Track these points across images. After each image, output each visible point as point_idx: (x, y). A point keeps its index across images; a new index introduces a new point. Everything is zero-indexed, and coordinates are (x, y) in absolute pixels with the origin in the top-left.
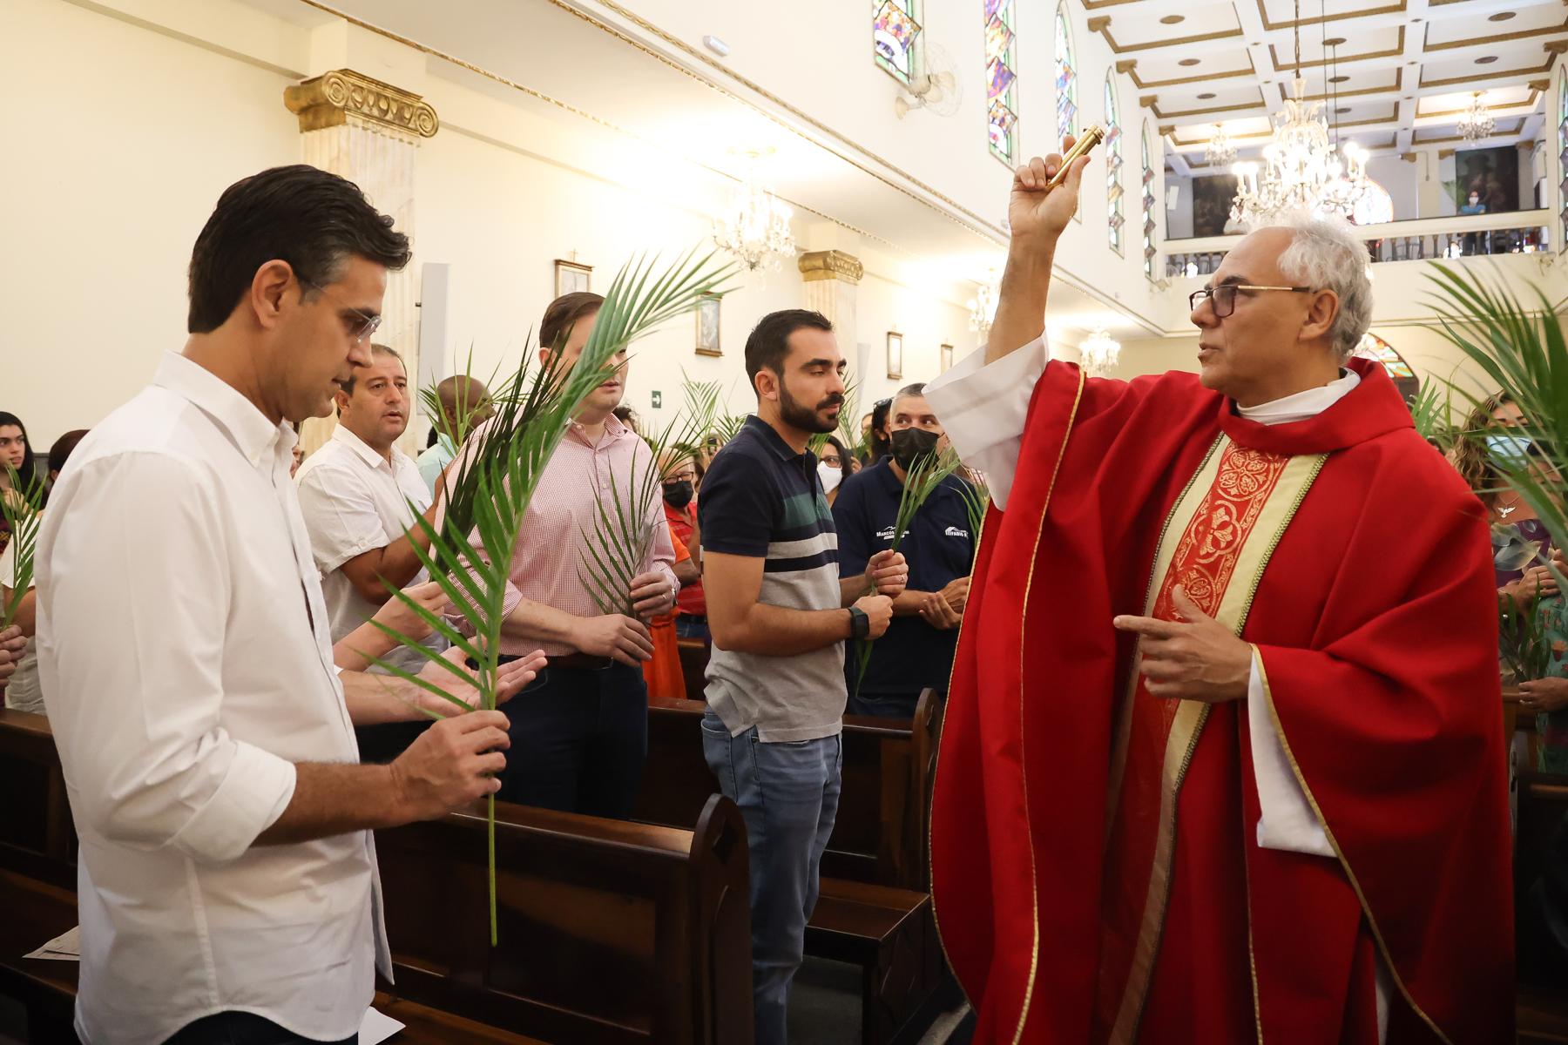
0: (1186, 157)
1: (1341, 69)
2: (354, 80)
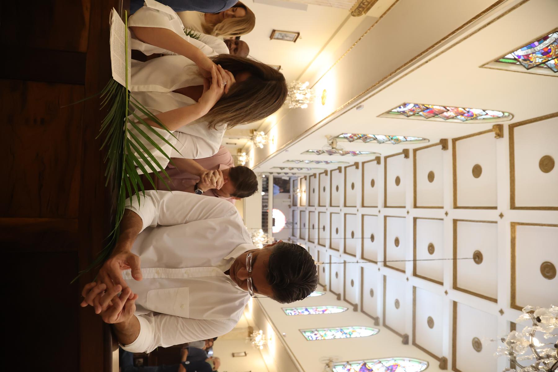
0: (297, 180)
1: (317, 230)
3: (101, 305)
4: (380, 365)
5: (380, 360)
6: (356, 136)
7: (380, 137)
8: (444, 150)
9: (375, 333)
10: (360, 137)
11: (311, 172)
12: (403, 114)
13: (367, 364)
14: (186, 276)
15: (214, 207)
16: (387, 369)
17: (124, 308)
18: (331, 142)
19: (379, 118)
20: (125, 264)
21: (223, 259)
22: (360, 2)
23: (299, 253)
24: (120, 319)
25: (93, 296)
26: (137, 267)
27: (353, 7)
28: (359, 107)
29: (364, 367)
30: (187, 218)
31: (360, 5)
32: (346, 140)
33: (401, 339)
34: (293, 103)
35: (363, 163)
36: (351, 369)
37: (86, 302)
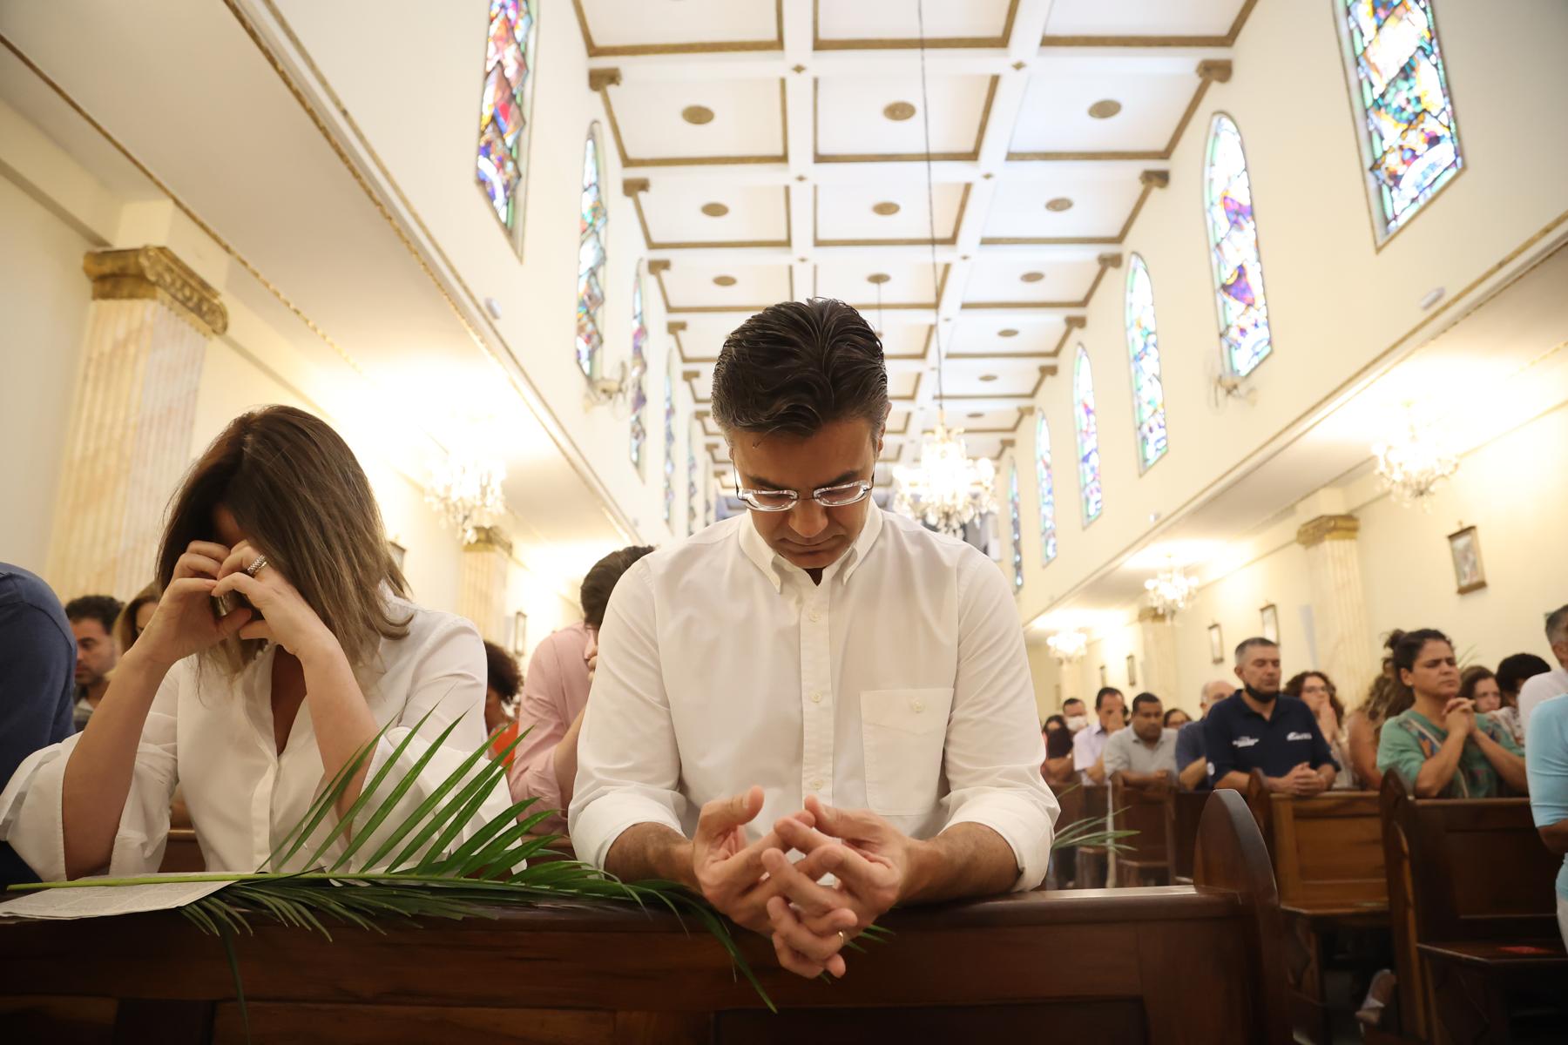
2: (165, 260)
3: (826, 910)
4: (1225, 244)
5: (1212, 245)
6: (585, 325)
7: (589, 256)
8: (620, 79)
9: (1141, 264)
10: (588, 312)
11: (702, 457)
12: (514, 190)
13: (1224, 281)
14: (828, 701)
15: (623, 621)
16: (1235, 225)
17: (856, 843)
18: (604, 397)
19: (526, 258)
20: (720, 846)
21: (781, 592)
22: (184, 309)
23: (733, 349)
24: (892, 858)
25: (804, 937)
26: (727, 806)
27: (198, 330)
28: (490, 313)
29: (1233, 290)
30: (655, 700)
31: (192, 310)
32: (598, 354)
33: (1156, 193)
34: (488, 504)
35: (670, 309)
36: (1238, 326)
37: (829, 959)
